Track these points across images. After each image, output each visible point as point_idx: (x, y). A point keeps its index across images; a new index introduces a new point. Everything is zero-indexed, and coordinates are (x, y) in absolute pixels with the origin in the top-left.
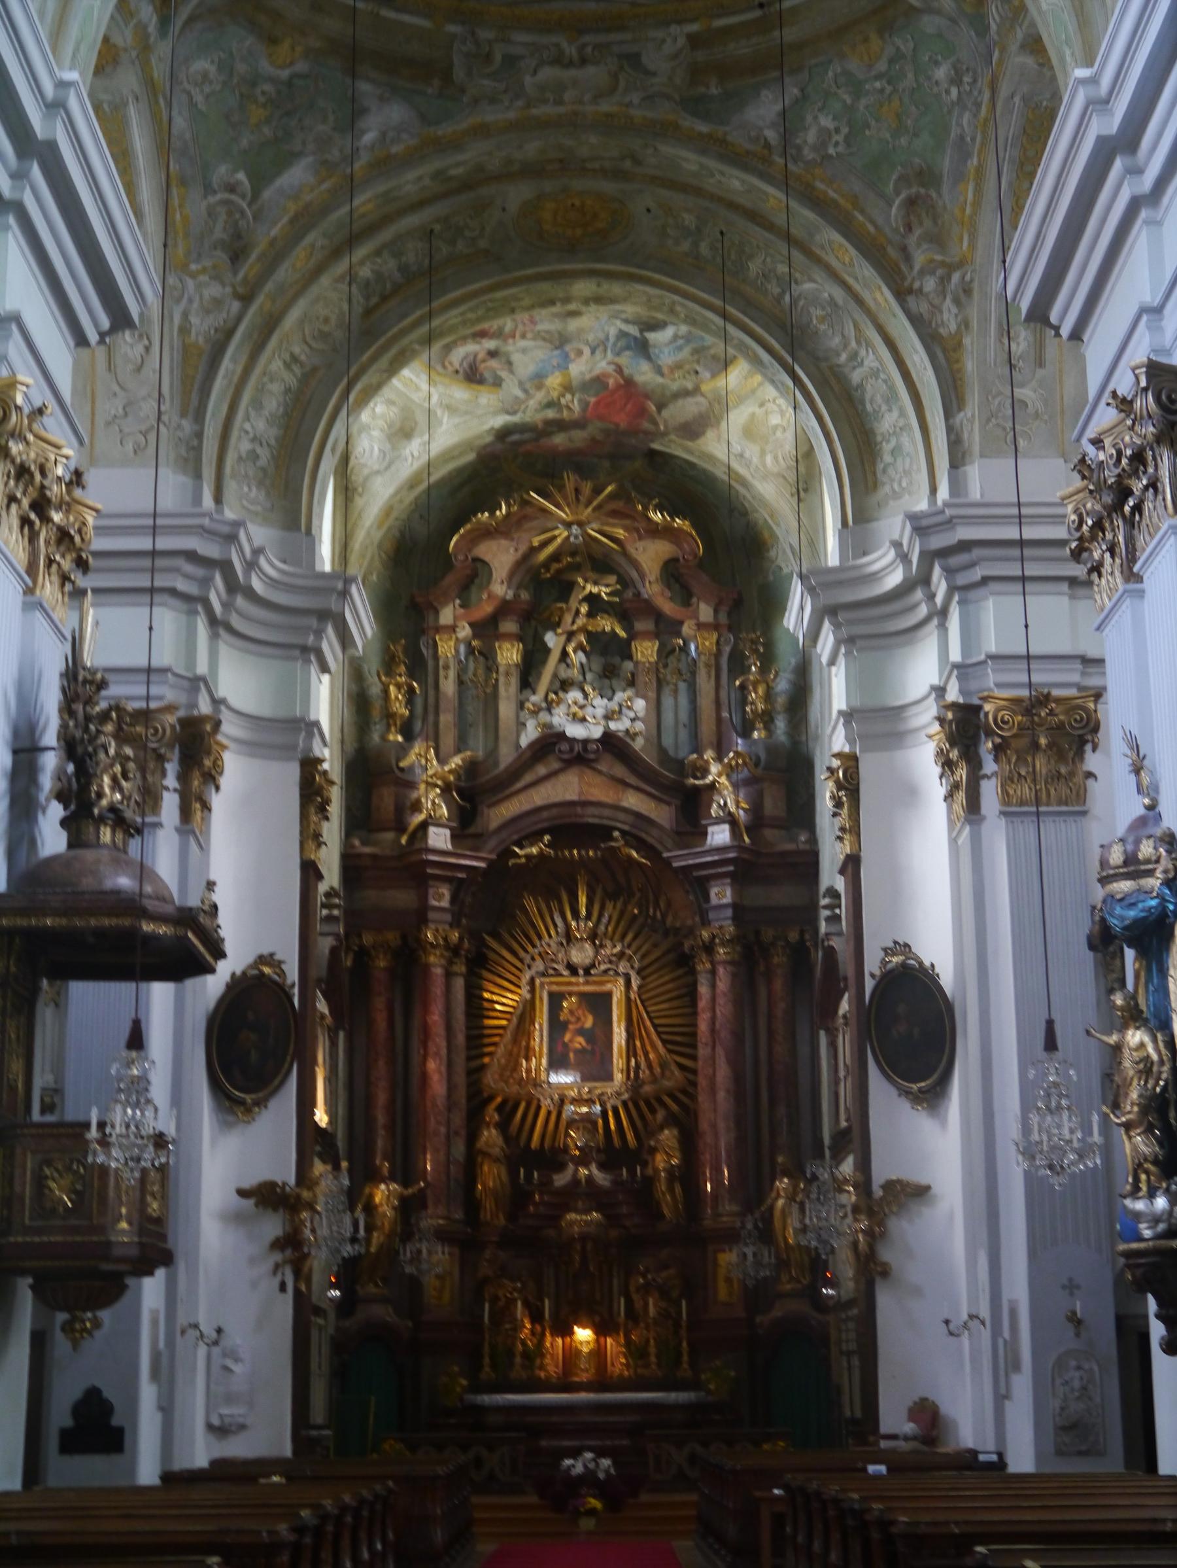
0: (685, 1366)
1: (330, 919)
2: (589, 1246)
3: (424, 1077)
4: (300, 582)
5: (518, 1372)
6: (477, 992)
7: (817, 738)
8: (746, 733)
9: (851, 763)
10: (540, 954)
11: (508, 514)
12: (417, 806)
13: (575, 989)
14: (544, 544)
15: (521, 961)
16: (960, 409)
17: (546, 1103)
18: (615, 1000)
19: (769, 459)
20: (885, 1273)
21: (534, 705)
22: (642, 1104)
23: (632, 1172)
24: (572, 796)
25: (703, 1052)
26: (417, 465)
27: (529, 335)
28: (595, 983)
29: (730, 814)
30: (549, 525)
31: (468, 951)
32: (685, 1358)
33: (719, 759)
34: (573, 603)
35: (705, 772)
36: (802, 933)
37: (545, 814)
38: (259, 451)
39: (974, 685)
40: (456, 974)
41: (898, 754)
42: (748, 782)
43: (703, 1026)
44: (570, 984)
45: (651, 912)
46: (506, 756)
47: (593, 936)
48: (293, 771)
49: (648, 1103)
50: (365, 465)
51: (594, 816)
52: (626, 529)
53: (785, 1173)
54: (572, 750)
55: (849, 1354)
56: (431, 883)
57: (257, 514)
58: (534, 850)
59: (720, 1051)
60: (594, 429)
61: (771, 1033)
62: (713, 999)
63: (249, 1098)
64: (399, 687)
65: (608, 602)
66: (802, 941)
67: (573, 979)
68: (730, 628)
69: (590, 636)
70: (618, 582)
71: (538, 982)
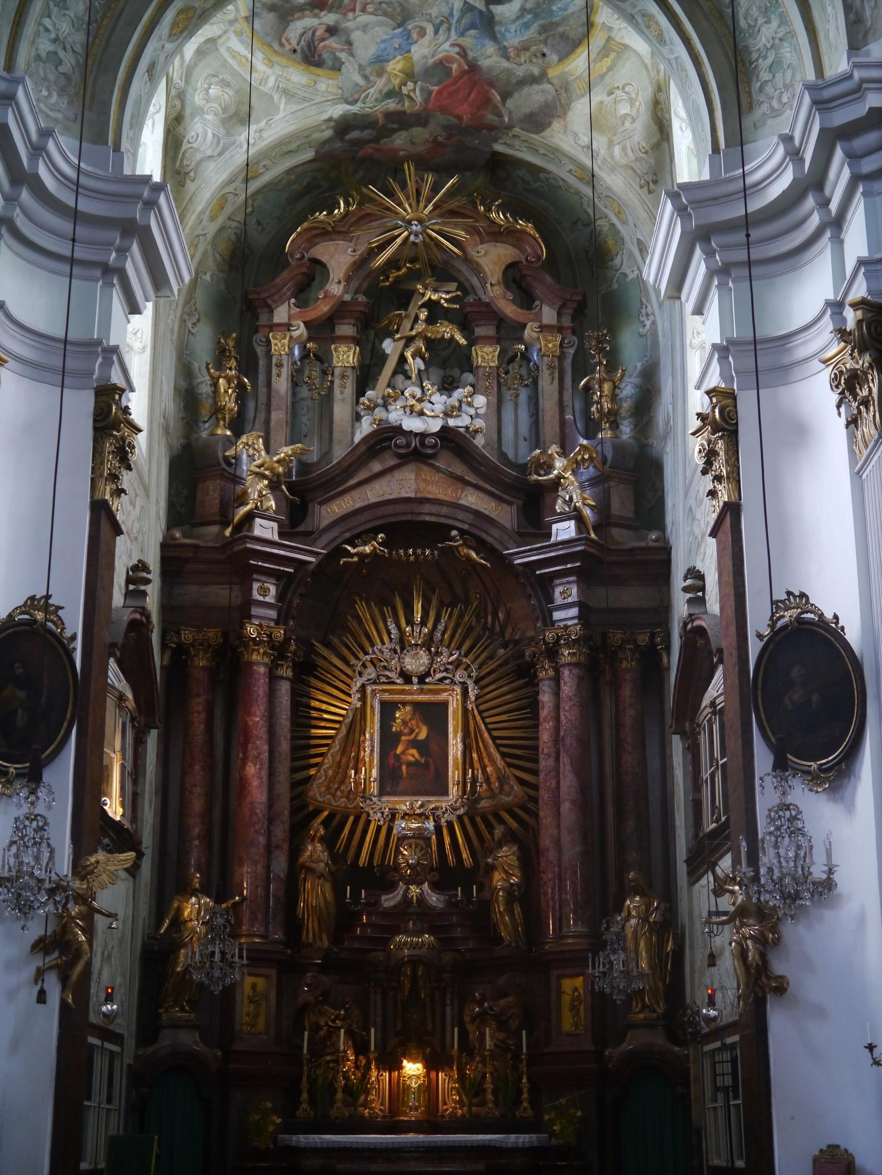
0: (525, 1104)
3: (243, 783)
5: (338, 1110)
6: (304, 700)
9: (729, 401)
10: (372, 661)
11: (347, 213)
12: (242, 499)
13: (409, 698)
14: (382, 247)
17: (376, 817)
19: (617, 150)
20: (781, 988)
21: (369, 400)
22: (478, 819)
23: (467, 893)
24: (408, 492)
25: (545, 763)
27: (370, 8)
28: (431, 692)
29: (576, 509)
31: (294, 653)
32: (525, 1096)
33: (564, 453)
34: (412, 310)
35: (550, 467)
36: (653, 636)
37: (380, 512)
38: (62, 54)
40: (282, 678)
42: (594, 482)
43: (545, 736)
44: (403, 692)
46: (339, 453)
47: (428, 643)
49: (484, 818)
50: (197, 150)
51: (431, 514)
53: (636, 891)
54: (408, 445)
58: (368, 549)
59: (565, 759)
61: (618, 744)
62: (557, 708)
64: (229, 380)
65: (447, 308)
66: (653, 645)
67: (407, 687)
68: (574, 333)
71: (369, 689)
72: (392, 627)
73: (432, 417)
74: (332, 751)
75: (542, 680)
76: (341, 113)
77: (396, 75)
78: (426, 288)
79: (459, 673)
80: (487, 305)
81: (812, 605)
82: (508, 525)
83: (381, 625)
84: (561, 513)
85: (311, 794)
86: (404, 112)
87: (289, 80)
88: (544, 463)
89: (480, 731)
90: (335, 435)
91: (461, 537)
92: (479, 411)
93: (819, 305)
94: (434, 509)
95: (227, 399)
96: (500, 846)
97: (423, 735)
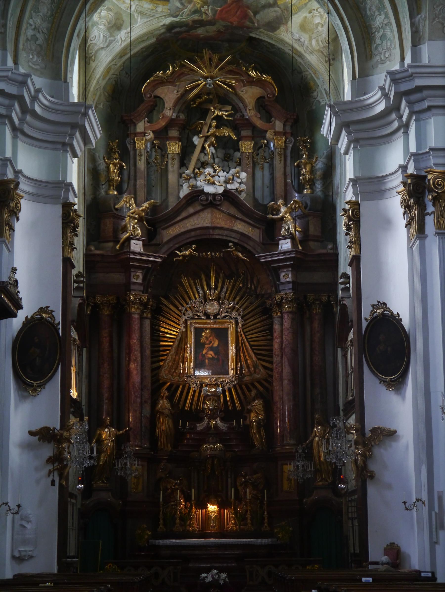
0: (266, 525)
1: (78, 289)
2: (216, 461)
3: (129, 372)
4: (61, 108)
7: (338, 193)
8: (300, 191)
9: (356, 207)
10: (190, 308)
11: (173, 72)
12: (124, 229)
13: (209, 326)
15: (180, 311)
16: (418, 13)
17: (193, 386)
18: (230, 332)
19: (314, 42)
20: (372, 476)
21: (187, 175)
22: (244, 386)
23: (238, 422)
25: (276, 359)
26: (124, 44)
28: (219, 323)
29: (291, 234)
30: (196, 78)
31: (152, 306)
32: (266, 521)
33: (286, 205)
34: (208, 121)
35: (279, 211)
36: (329, 297)
37: (193, 234)
38: (38, 35)
39: (422, 165)
40: (146, 318)
41: (381, 202)
42: (301, 217)
43: (276, 346)
44: (206, 323)
45: (249, 286)
46: (172, 203)
48: (58, 210)
50: (95, 44)
51: (219, 235)
52: (237, 80)
54: (207, 200)
55: (352, 519)
56: (132, 270)
57: (37, 70)
58: (187, 253)
59: (285, 360)
60: (220, 25)
62: (282, 331)
63: (35, 383)
64: (115, 165)
65: (226, 120)
66: (329, 301)
67: (208, 321)
68: (292, 135)
69: (217, 138)
70: (232, 110)
71: (189, 322)
72: (200, 290)
73: (219, 185)
74: (171, 353)
75: (275, 317)
76: (170, 22)
77: (198, 3)
78: (215, 109)
79: (233, 313)
80: (247, 119)
81: (388, 308)
82: (257, 239)
83: (195, 289)
84: (284, 236)
85: (161, 375)
86: (203, 20)
87: (142, 7)
88: (276, 208)
89: (244, 342)
90: (170, 190)
91: (234, 246)
92: (243, 181)
93: (395, 167)
94: (220, 232)
95: (114, 175)
96: (254, 400)
97: (216, 344)
